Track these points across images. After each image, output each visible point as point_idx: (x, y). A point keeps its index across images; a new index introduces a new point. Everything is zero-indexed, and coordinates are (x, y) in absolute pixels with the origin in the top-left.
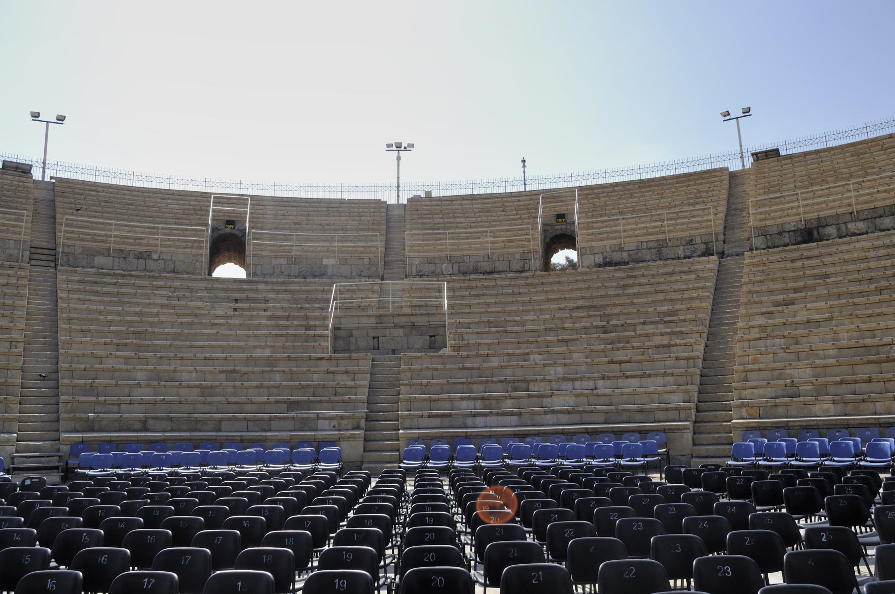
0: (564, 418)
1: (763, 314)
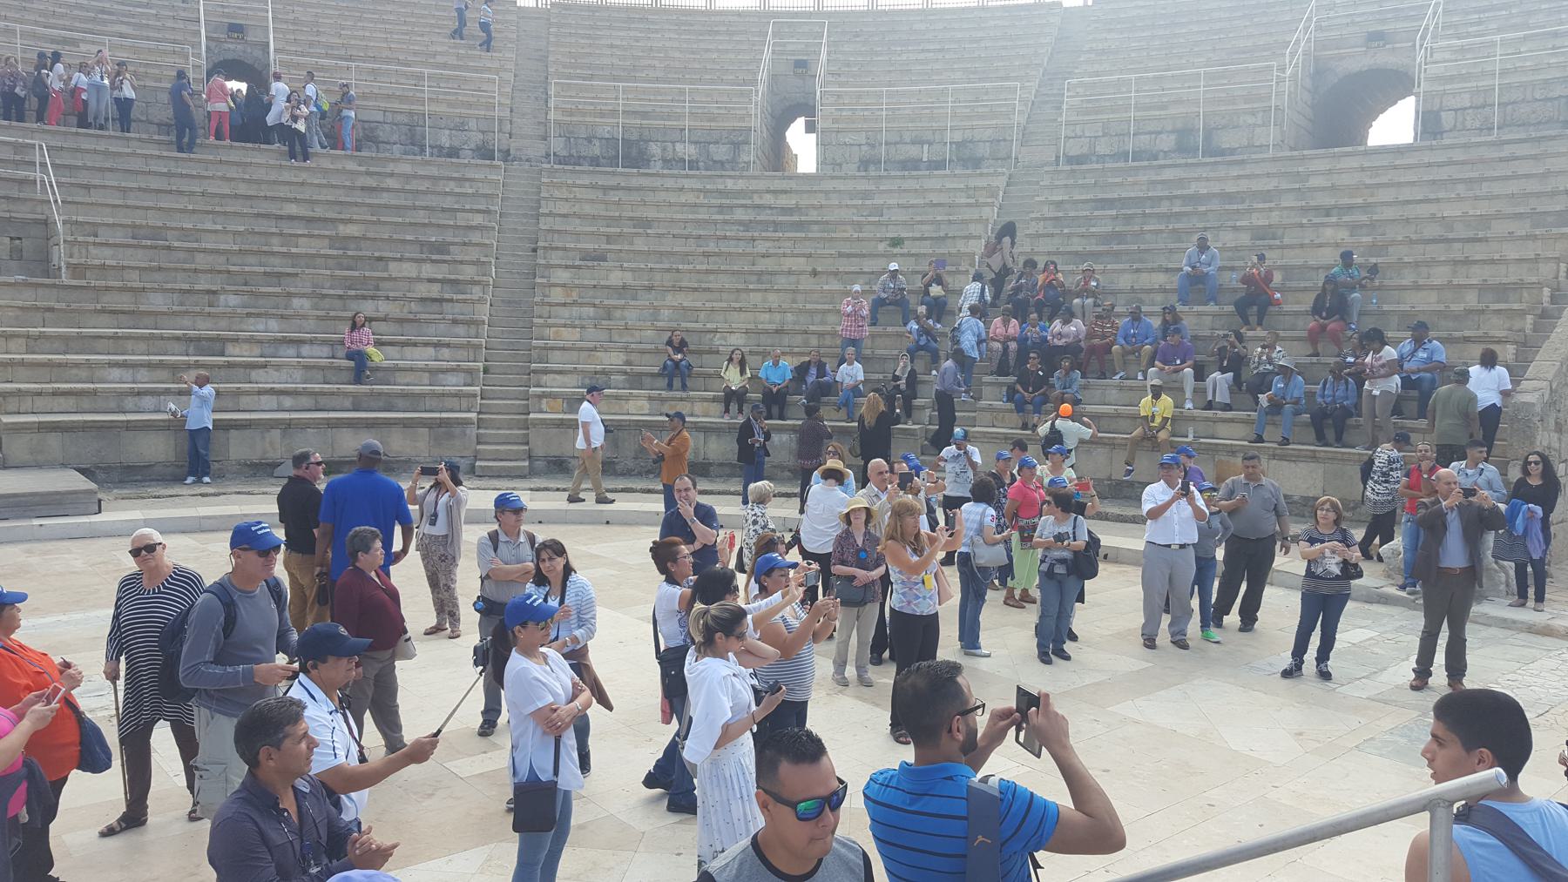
0: (288, 402)
1: (567, 267)
